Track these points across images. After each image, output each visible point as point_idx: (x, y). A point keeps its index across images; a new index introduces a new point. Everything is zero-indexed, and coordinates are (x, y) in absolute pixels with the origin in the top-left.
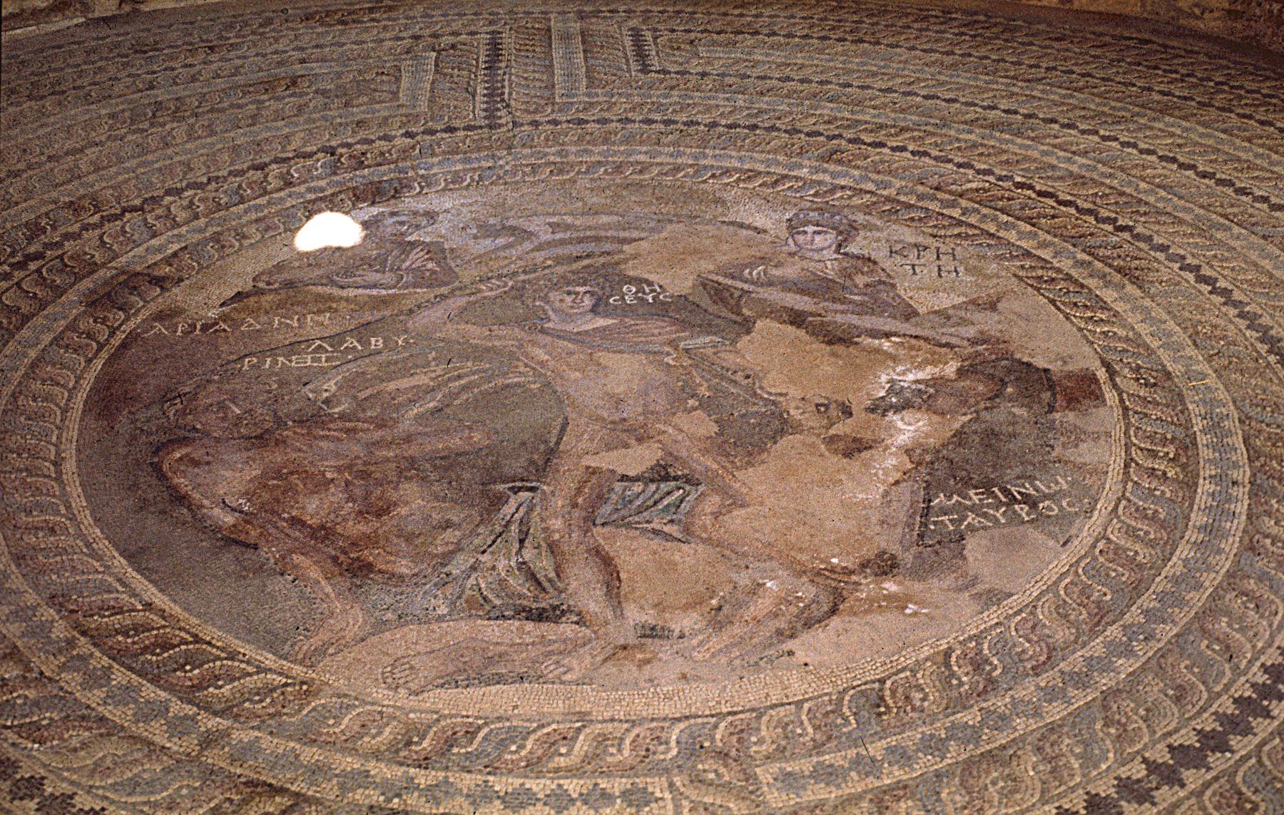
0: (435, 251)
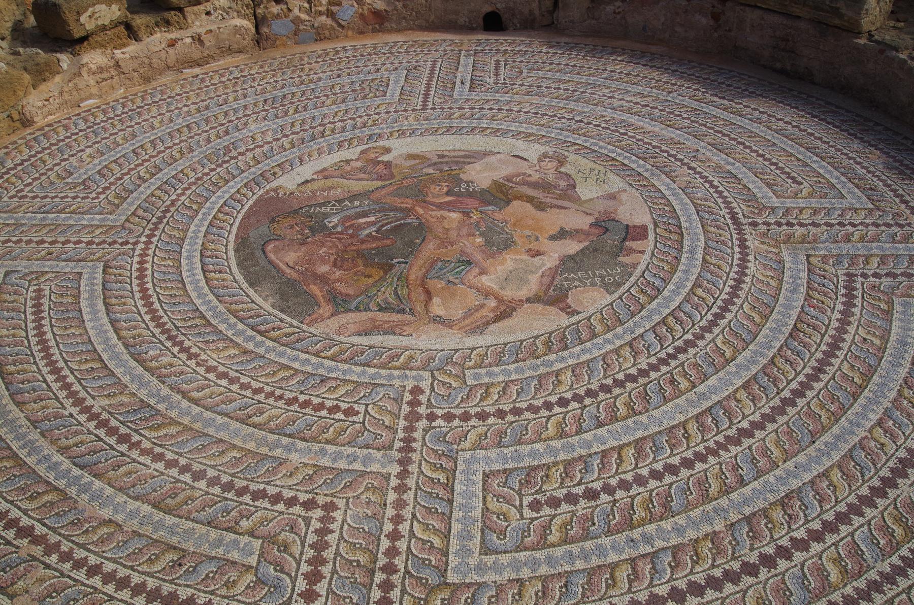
0: (388, 165)
